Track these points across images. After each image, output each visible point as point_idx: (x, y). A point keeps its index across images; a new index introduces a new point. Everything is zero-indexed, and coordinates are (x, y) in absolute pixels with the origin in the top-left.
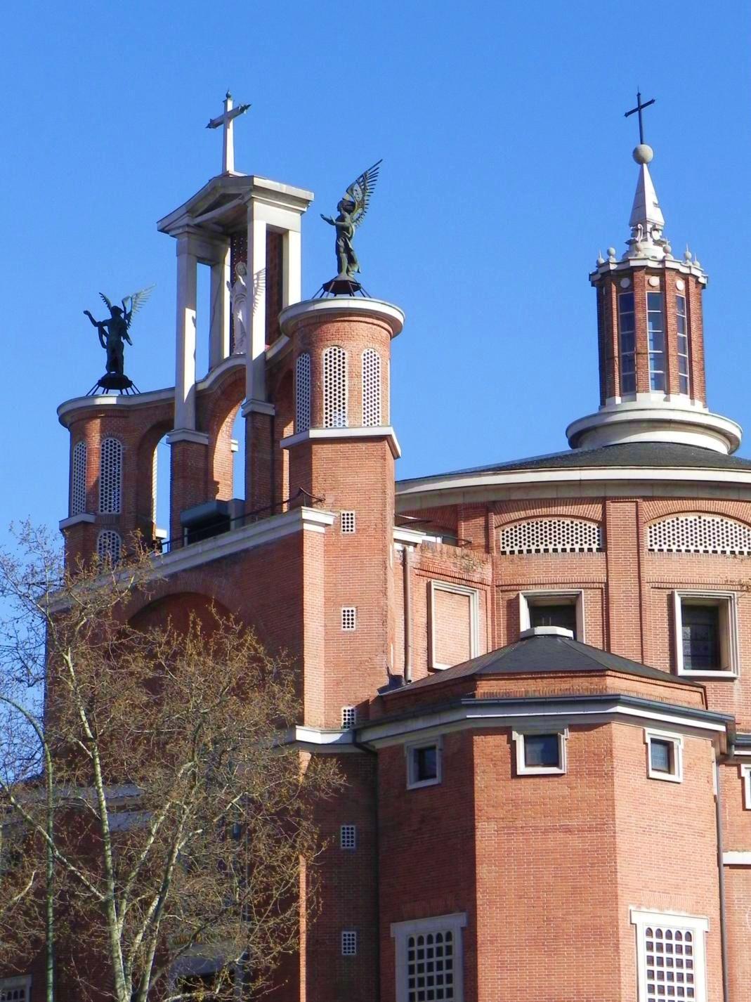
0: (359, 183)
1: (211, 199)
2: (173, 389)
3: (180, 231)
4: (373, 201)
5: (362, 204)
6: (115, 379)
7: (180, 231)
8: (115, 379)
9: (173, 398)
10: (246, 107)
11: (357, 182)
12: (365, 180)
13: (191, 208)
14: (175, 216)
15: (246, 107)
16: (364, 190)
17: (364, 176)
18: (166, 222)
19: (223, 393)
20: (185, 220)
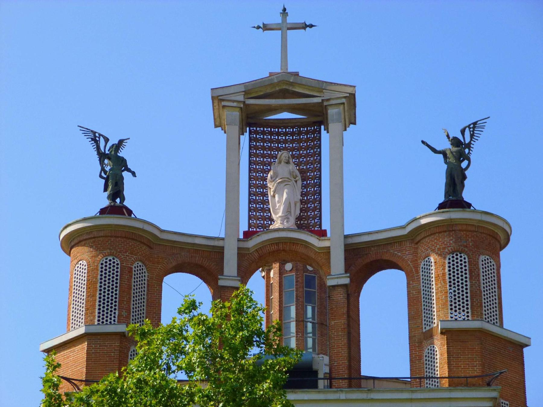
0: (470, 128)
1: (269, 91)
2: (223, 239)
3: (235, 104)
4: (476, 145)
5: (469, 146)
6: (116, 208)
7: (235, 104)
8: (116, 208)
9: (223, 248)
10: (311, 26)
11: (469, 126)
12: (474, 127)
13: (251, 90)
14: (232, 90)
15: (311, 26)
16: (472, 136)
17: (475, 124)
18: (220, 92)
19: (260, 257)
20: (241, 98)
